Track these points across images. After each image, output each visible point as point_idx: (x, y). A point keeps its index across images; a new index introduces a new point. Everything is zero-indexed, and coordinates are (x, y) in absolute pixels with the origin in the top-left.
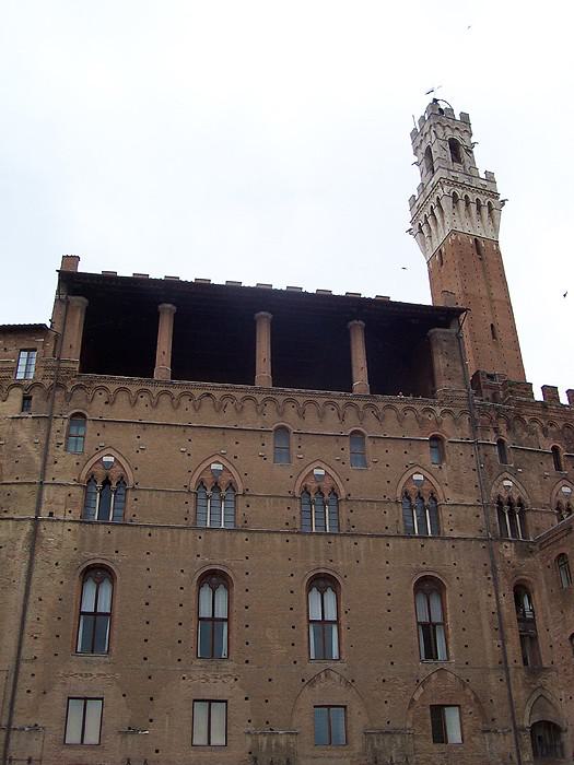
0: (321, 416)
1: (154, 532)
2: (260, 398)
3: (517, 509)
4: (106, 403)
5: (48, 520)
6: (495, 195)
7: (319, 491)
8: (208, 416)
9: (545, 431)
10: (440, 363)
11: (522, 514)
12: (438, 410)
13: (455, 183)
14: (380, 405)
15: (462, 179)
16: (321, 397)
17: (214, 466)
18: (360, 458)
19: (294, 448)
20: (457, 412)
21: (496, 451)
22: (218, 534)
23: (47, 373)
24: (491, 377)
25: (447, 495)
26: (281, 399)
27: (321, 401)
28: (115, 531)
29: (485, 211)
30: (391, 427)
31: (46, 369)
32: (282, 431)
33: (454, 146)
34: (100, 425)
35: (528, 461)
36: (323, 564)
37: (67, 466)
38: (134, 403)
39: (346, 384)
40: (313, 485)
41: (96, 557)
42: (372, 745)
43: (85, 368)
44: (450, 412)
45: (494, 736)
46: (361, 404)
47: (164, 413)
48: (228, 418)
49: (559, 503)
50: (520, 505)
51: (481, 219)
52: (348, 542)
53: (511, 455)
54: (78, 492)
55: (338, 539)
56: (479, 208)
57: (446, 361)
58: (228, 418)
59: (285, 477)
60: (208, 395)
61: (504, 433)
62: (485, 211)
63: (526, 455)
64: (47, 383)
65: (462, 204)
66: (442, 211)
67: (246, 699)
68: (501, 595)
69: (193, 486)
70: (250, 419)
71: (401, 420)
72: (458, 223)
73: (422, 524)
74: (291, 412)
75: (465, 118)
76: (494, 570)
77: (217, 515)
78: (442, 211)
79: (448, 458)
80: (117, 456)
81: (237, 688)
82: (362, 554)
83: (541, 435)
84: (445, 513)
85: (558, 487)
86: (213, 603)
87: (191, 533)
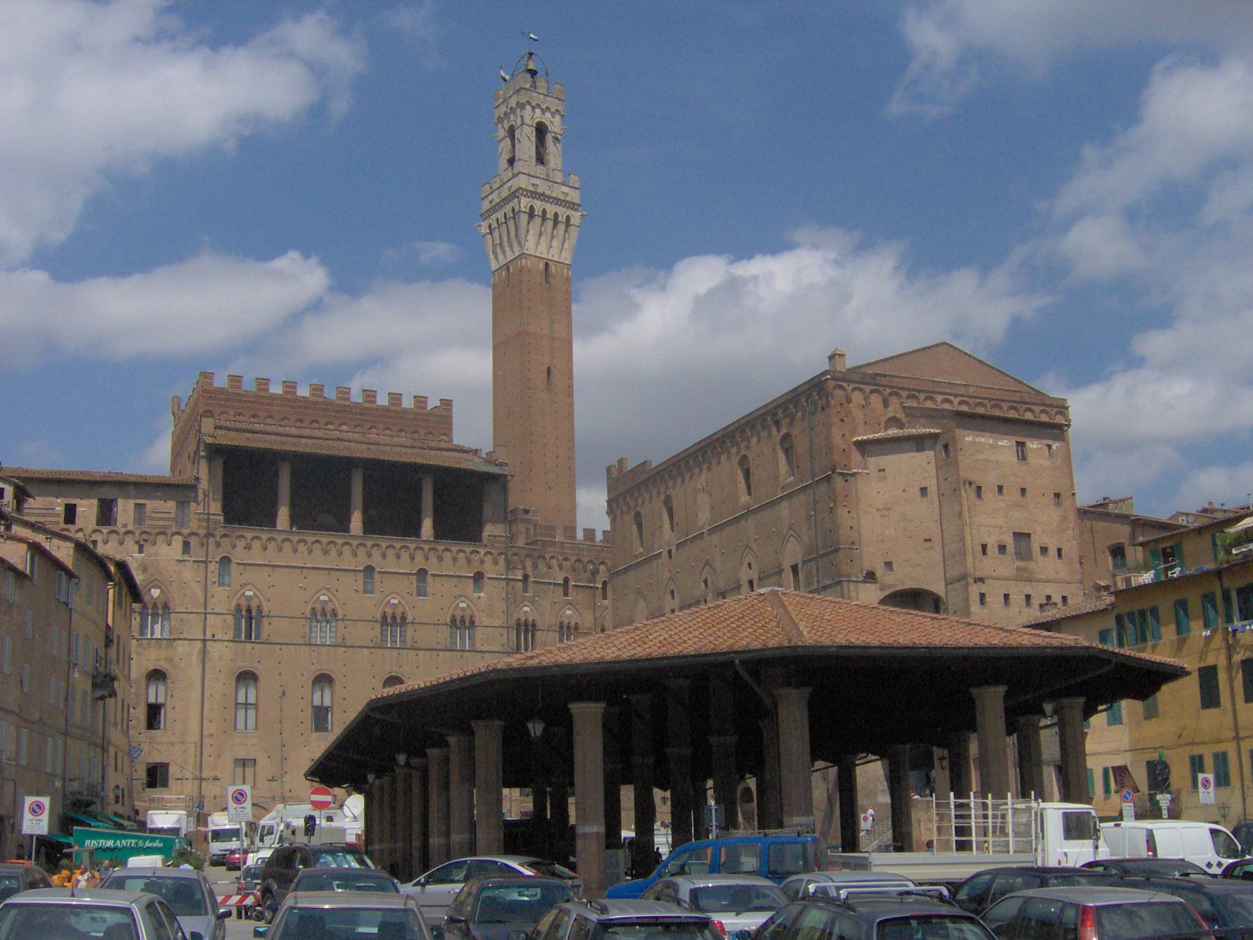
7: (394, 617)
12: (482, 551)
15: (543, 188)
17: (322, 598)
18: (421, 592)
19: (377, 584)
20: (495, 552)
24: (527, 512)
25: (481, 619)
27: (398, 545)
28: (257, 647)
29: (562, 227)
32: (369, 570)
37: (221, 599)
40: (389, 611)
41: (246, 666)
46: (426, 547)
47: (286, 557)
48: (332, 561)
50: (534, 625)
53: (531, 587)
54: (230, 618)
58: (332, 561)
59: (370, 606)
64: (202, 532)
69: (308, 613)
70: (348, 561)
73: (463, 644)
74: (377, 554)
77: (323, 634)
87: (308, 648)
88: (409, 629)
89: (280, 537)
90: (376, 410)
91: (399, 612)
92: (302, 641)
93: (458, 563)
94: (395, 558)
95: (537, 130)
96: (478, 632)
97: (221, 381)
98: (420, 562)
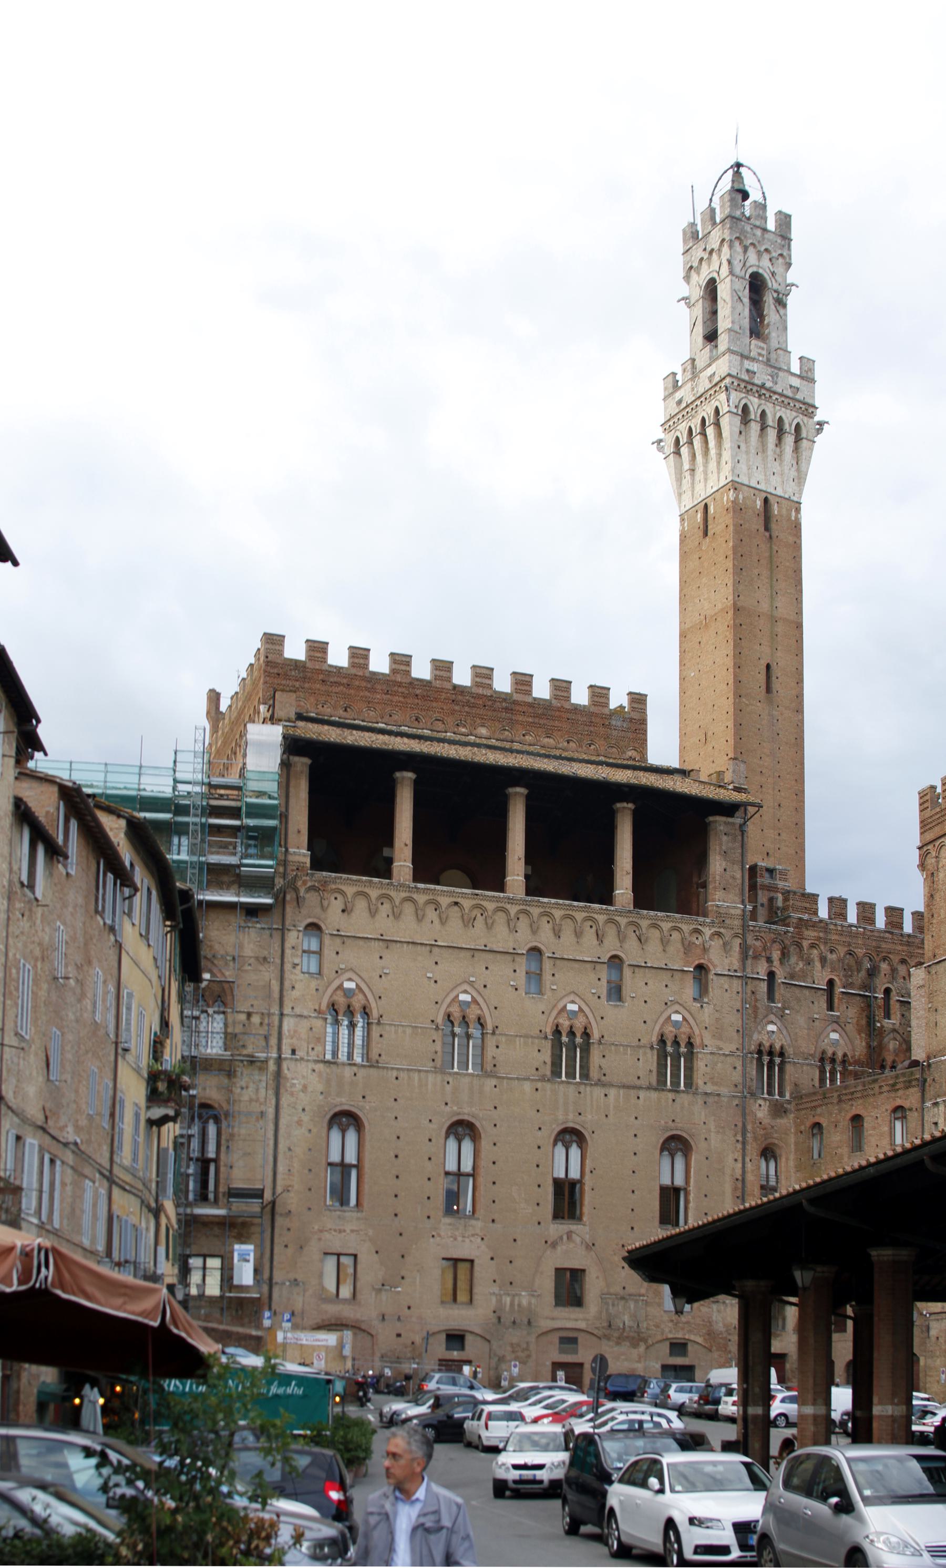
0: (578, 934)
1: (402, 1075)
2: (513, 910)
3: (777, 1060)
5: (291, 1059)
6: (808, 409)
8: (455, 933)
9: (823, 960)
10: (717, 865)
11: (782, 1064)
13: (747, 385)
14: (644, 923)
15: (762, 376)
16: (580, 910)
18: (616, 992)
19: (547, 977)
21: (764, 987)
22: (467, 1080)
26: (535, 911)
29: (789, 440)
30: (654, 954)
33: (757, 285)
34: (338, 941)
36: (571, 1117)
38: (373, 913)
39: (605, 896)
40: (565, 1023)
42: (607, 1310)
43: (317, 864)
44: (719, 934)
45: (722, 1307)
46: (623, 921)
47: (407, 928)
48: (477, 936)
49: (824, 1052)
50: (782, 1054)
51: (779, 457)
52: (598, 1092)
53: (780, 992)
56: (781, 432)
57: (724, 864)
58: (477, 936)
60: (456, 903)
61: (776, 963)
62: (789, 440)
63: (797, 991)
65: (755, 427)
66: (719, 434)
67: (492, 1259)
68: (747, 1159)
70: (501, 938)
71: (665, 942)
72: (743, 467)
74: (546, 930)
75: (785, 220)
76: (744, 1131)
78: (719, 434)
79: (711, 994)
81: (483, 1247)
82: (612, 1106)
83: (818, 965)
84: (700, 1065)
85: (825, 1034)
86: (458, 1156)
89: (398, 896)
90: (530, 705)
91: (579, 1024)
93: (671, 949)
94: (574, 932)
95: (751, 284)
97: (295, 651)
98: (611, 946)
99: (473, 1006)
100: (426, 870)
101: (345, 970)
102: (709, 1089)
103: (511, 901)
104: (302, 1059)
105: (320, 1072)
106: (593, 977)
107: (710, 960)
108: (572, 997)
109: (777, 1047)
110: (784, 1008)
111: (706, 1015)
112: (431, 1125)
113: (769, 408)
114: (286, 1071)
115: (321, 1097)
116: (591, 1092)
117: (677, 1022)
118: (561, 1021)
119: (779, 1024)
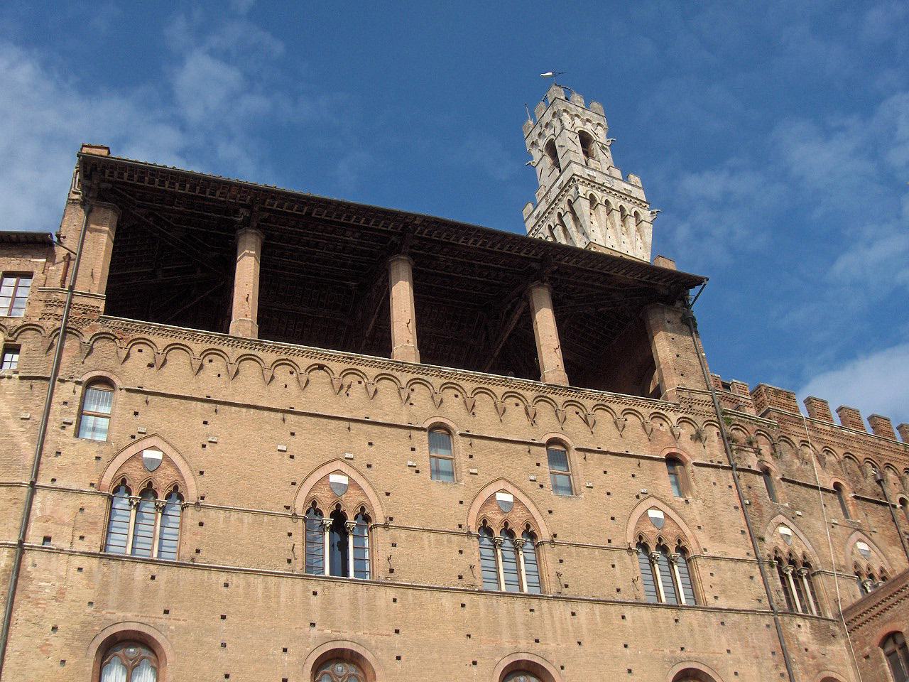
1: (235, 579)
2: (405, 378)
4: (151, 366)
5: (41, 549)
8: (320, 396)
9: (820, 459)
12: (673, 417)
14: (589, 404)
17: (334, 478)
19: (462, 459)
20: (700, 421)
23: (52, 310)
30: (606, 435)
31: (48, 303)
34: (139, 398)
35: (808, 502)
36: (523, 644)
37: (78, 461)
41: (131, 620)
46: (560, 400)
47: (249, 385)
48: (355, 403)
49: (856, 565)
50: (807, 565)
52: (561, 609)
53: (782, 490)
54: (97, 505)
55: (545, 604)
56: (624, 217)
59: (451, 503)
69: (300, 508)
70: (388, 405)
79: (695, 488)
80: (169, 451)
83: (816, 464)
88: (548, 554)
89: (234, 352)
92: (284, 568)
93: (629, 433)
96: (703, 570)
99: (351, 491)
100: (275, 323)
101: (145, 435)
102: (722, 603)
103: (401, 366)
104: (61, 551)
105: (91, 571)
106: (528, 461)
107: (683, 449)
108: (501, 485)
109: (798, 553)
110: (793, 509)
111: (696, 512)
112: (286, 657)
113: (611, 199)
114: (29, 569)
115: (89, 610)
116: (550, 608)
117: (657, 519)
118: (489, 514)
119: (792, 527)
